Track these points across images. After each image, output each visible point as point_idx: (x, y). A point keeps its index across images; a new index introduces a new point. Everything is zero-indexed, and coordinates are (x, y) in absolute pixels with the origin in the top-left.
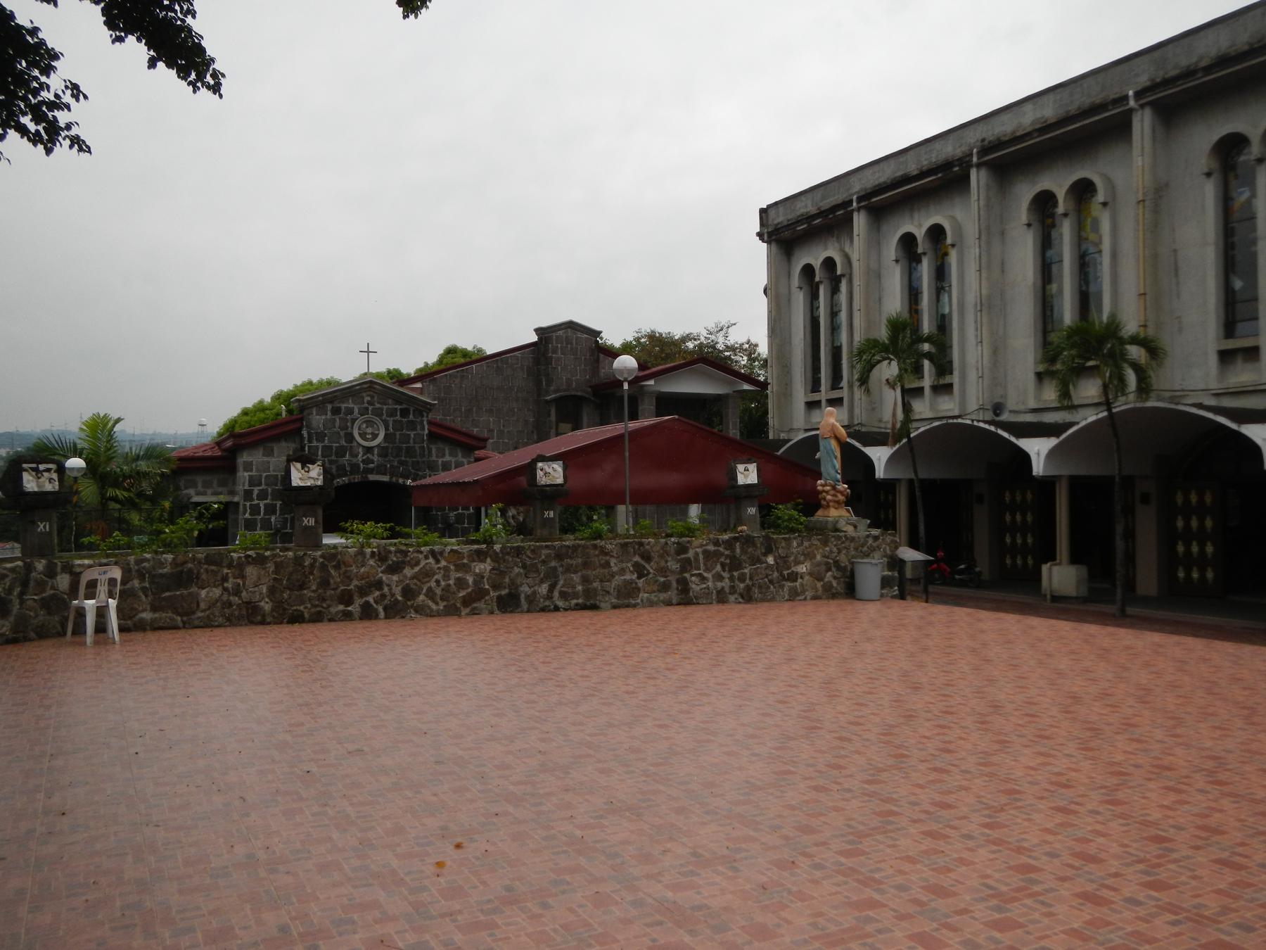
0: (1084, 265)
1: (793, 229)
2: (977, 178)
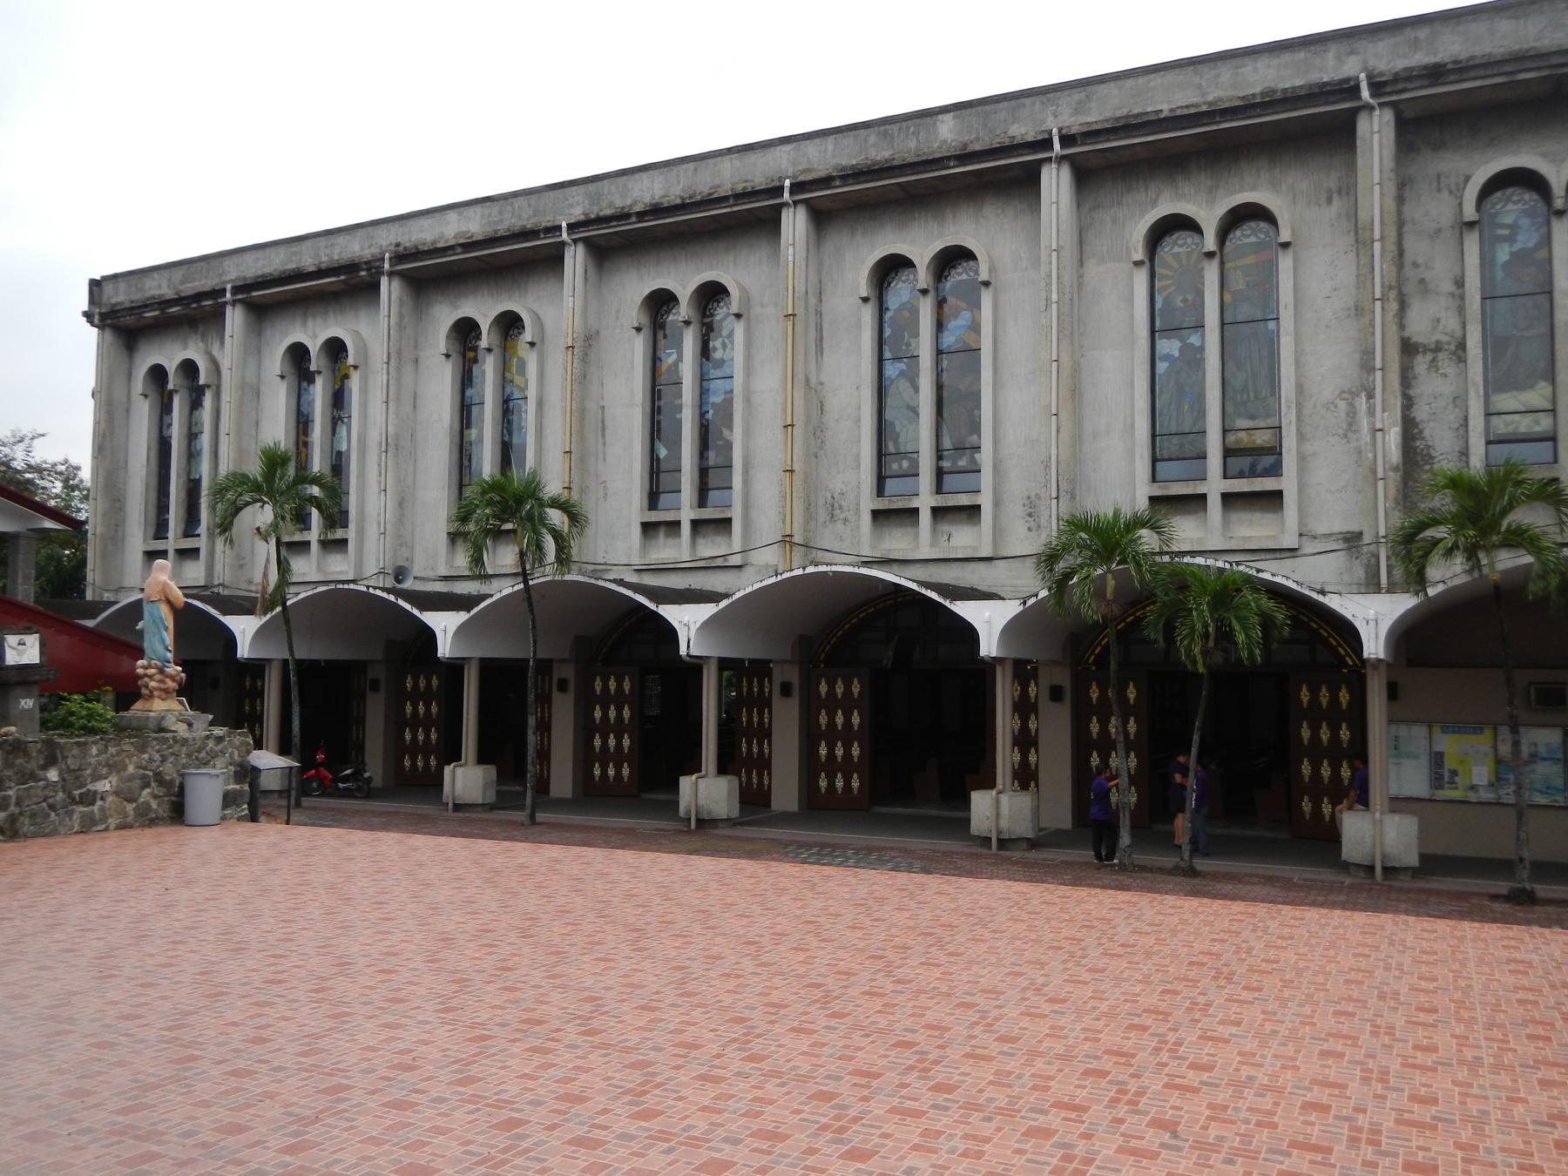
0: (508, 410)
1: (141, 317)
2: (389, 289)
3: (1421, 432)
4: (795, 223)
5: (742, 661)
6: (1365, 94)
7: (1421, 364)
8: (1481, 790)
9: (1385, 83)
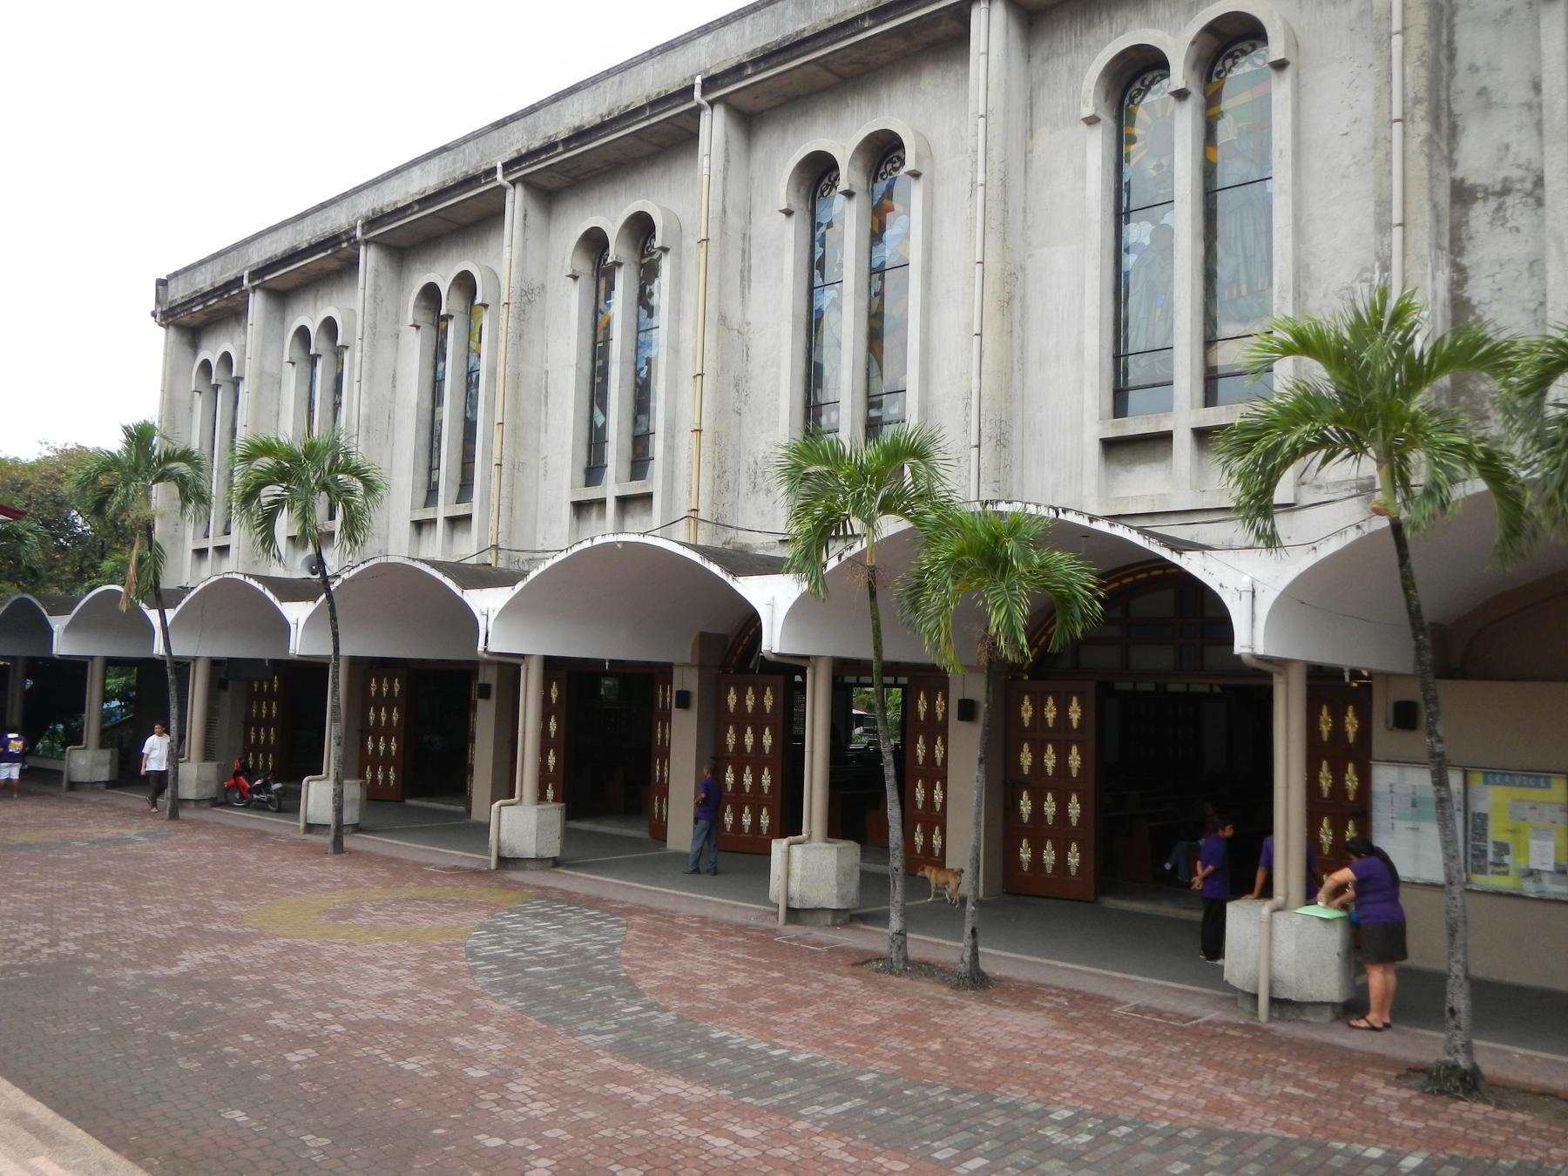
0: (471, 381)
1: (198, 314)
2: (369, 259)
4: (714, 127)
5: (262, 661)
7: (1479, 216)
8: (1546, 878)
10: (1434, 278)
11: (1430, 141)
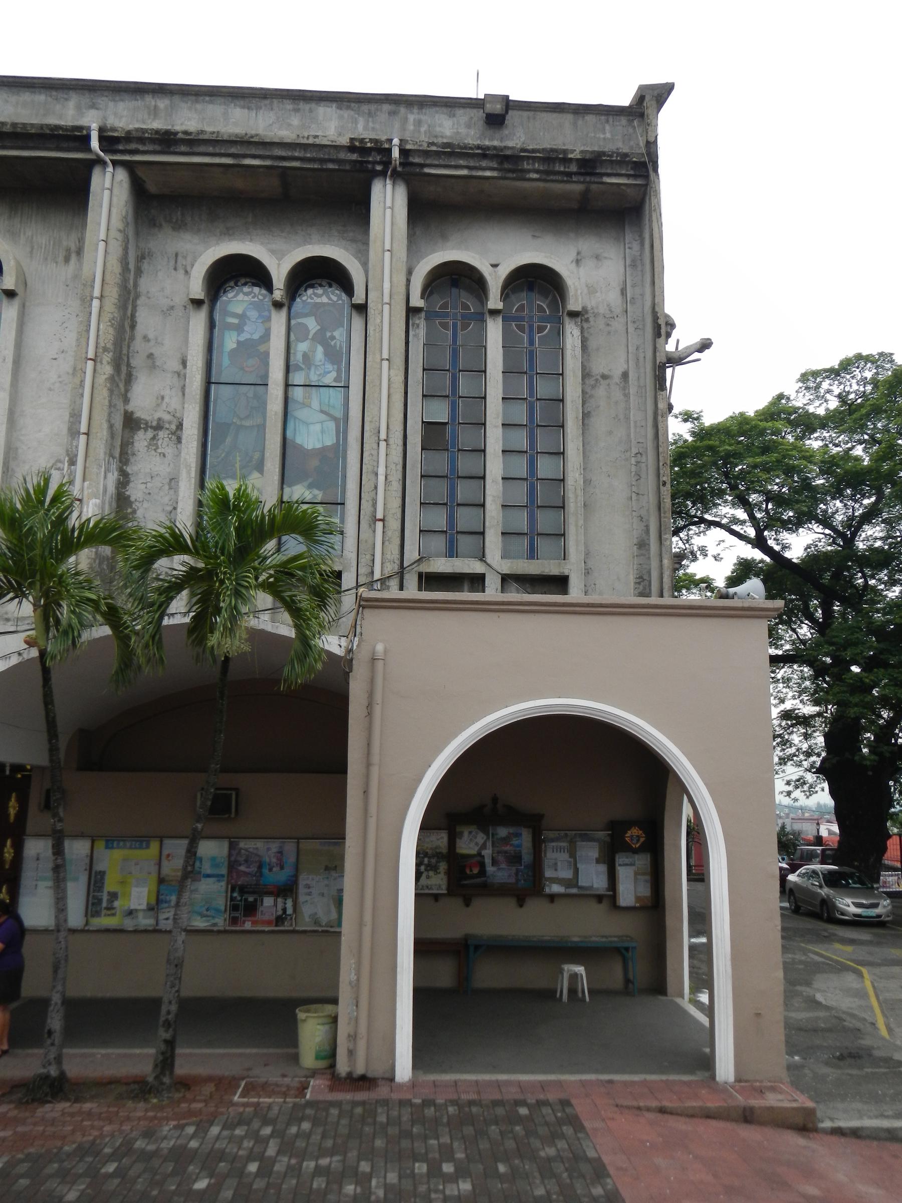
3: (134, 512)
6: (95, 144)
7: (141, 440)
8: (141, 915)
9: (117, 140)
10: (105, 477)
11: (112, 379)
